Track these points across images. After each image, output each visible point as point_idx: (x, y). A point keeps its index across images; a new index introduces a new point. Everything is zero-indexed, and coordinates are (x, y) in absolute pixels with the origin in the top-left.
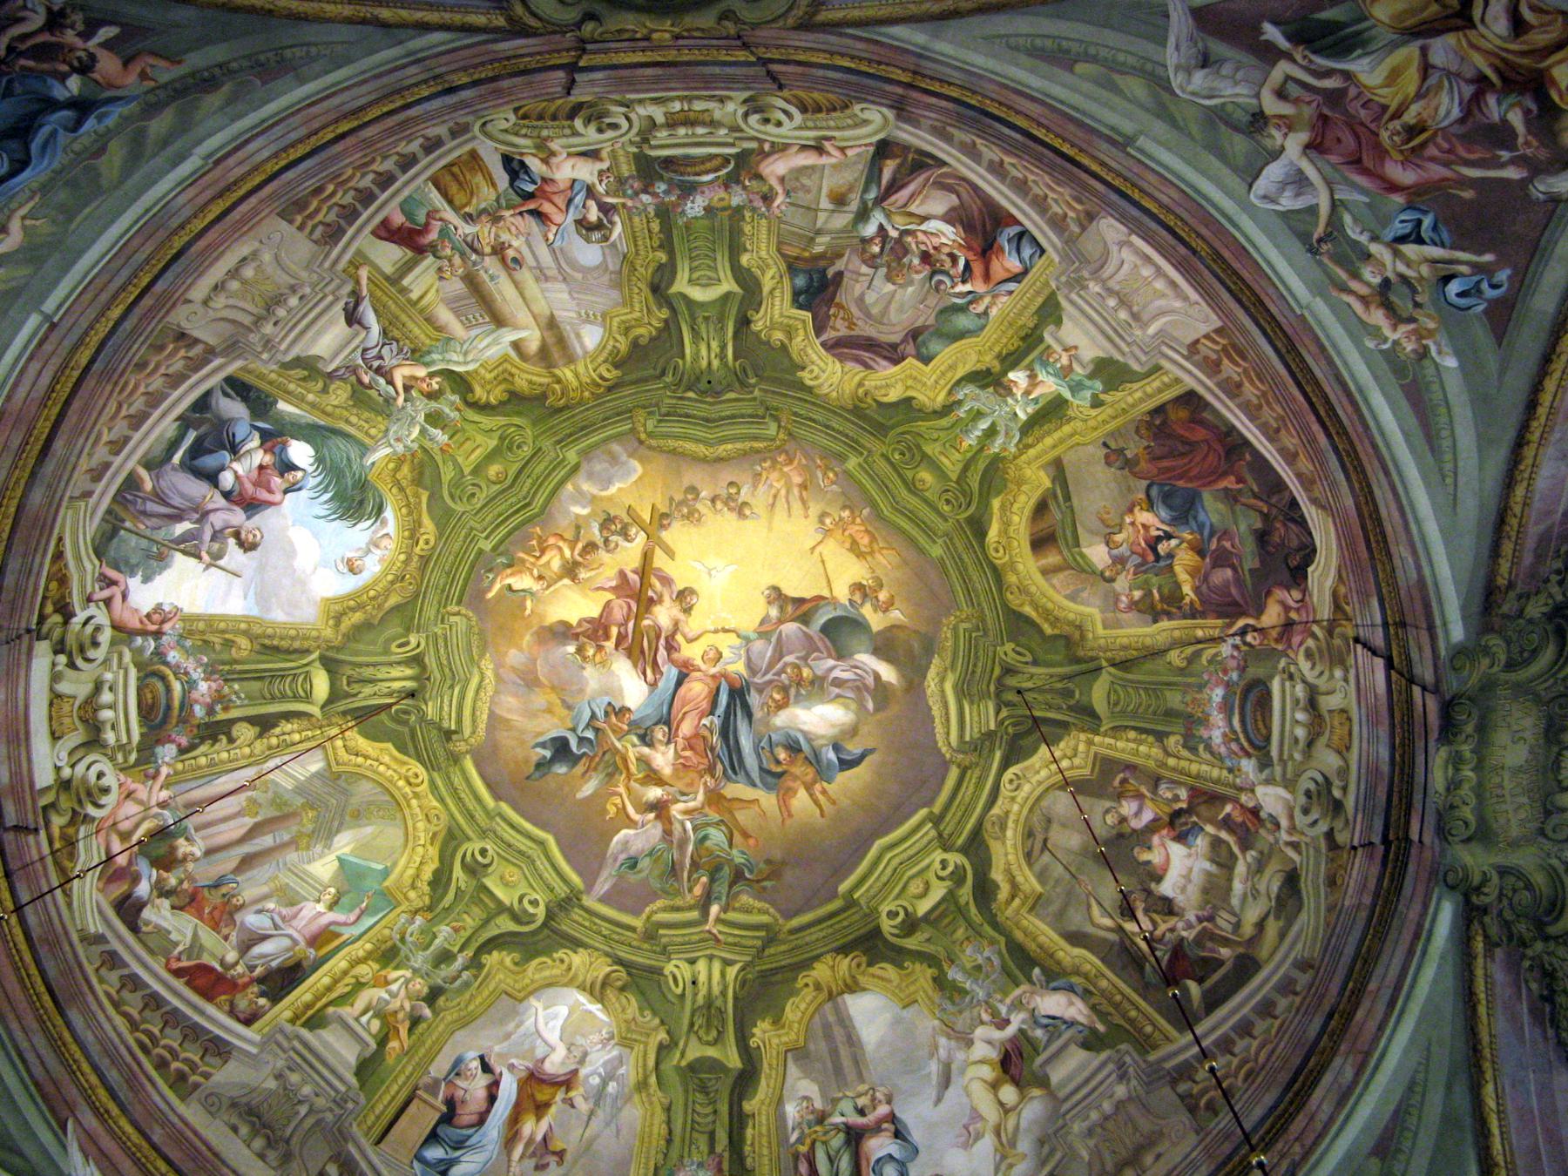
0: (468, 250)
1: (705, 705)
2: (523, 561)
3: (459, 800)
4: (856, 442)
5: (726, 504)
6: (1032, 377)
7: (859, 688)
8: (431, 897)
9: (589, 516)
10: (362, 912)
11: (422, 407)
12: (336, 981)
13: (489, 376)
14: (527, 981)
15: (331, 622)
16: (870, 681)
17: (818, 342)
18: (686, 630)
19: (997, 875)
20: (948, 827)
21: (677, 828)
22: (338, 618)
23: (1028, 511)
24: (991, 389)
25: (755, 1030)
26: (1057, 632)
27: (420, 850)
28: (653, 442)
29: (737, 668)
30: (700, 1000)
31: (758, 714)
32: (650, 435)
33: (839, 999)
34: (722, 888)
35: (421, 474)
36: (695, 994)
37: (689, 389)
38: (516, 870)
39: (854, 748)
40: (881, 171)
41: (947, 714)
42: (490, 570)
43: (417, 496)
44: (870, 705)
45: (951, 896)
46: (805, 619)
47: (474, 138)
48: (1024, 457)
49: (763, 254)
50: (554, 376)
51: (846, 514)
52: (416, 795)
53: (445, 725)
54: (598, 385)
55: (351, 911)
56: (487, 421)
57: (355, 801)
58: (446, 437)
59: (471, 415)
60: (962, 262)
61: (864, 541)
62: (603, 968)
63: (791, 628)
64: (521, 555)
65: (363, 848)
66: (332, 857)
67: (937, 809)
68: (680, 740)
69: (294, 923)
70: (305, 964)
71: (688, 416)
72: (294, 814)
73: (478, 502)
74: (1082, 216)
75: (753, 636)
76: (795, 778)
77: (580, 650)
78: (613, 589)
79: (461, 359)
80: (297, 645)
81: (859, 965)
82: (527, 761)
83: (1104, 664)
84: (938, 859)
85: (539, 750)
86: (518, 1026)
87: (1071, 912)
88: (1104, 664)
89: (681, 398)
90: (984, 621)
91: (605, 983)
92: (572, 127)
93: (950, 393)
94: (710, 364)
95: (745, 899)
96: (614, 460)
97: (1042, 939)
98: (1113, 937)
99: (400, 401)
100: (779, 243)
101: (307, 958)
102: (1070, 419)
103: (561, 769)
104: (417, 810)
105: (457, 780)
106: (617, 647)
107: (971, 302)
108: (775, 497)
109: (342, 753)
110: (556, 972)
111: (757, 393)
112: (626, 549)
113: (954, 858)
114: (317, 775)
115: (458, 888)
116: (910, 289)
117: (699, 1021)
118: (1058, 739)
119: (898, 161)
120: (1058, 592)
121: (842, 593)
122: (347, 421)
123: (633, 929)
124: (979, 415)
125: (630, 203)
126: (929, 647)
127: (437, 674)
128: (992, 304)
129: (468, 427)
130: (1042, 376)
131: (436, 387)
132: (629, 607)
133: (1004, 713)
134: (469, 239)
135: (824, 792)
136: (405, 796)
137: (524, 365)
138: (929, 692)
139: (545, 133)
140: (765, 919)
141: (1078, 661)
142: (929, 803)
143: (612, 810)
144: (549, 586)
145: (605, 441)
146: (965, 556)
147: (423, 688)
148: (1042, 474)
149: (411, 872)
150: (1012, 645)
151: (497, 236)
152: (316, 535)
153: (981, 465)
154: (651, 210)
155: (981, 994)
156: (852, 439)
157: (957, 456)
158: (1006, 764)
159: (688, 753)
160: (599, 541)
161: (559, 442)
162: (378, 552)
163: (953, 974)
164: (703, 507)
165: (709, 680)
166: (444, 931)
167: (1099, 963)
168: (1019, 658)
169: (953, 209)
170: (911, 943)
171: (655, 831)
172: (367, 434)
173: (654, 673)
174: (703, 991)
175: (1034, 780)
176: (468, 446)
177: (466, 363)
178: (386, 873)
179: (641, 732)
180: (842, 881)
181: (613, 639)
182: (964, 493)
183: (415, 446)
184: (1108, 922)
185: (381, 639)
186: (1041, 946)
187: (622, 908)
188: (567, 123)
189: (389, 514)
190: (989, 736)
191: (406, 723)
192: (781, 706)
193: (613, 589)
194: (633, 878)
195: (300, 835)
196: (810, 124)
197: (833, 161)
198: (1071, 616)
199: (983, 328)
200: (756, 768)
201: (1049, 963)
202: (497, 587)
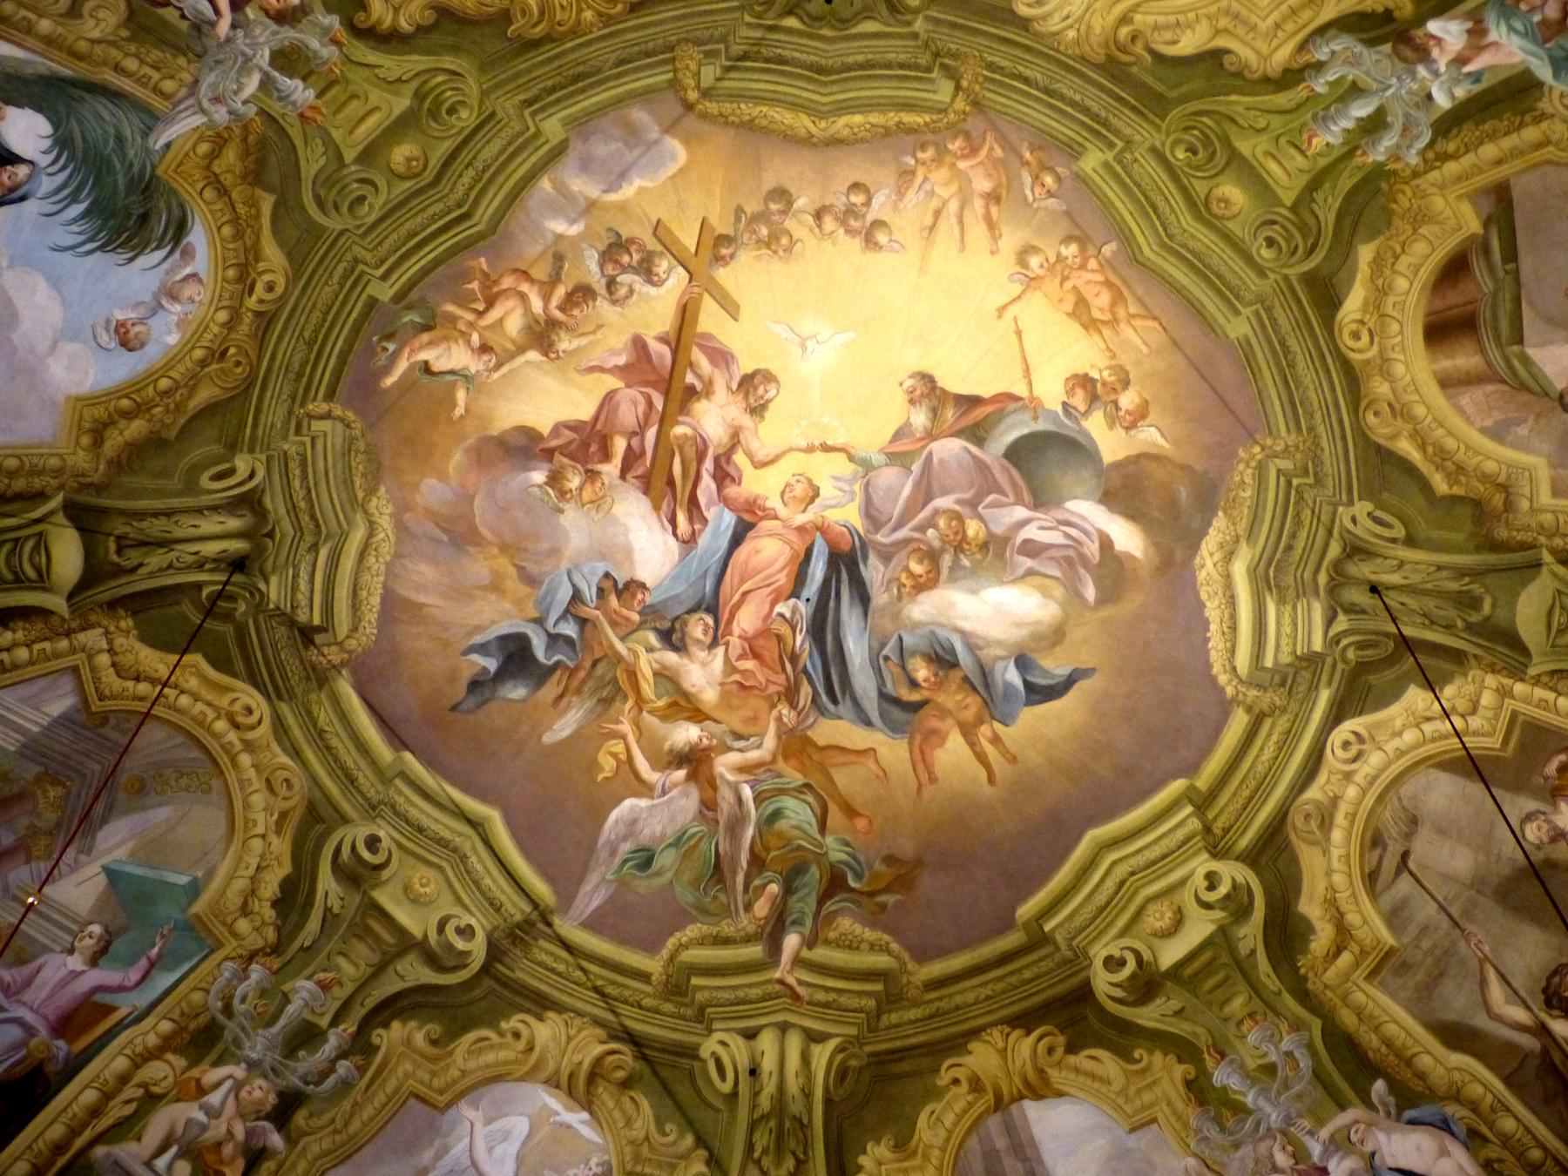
1: (783, 580)
2: (453, 319)
3: (327, 750)
5: (843, 222)
6: (1477, 32)
7: (1071, 561)
8: (279, 929)
9: (581, 237)
10: (152, 965)
11: (265, 38)
12: (107, 1097)
14: (456, 1073)
15: (86, 440)
16: (1092, 549)
18: (754, 445)
19: (1310, 907)
20: (1224, 809)
21: (726, 797)
22: (98, 433)
23: (1427, 272)
24: (1387, 48)
25: (863, 1160)
26: (1458, 491)
27: (257, 844)
28: (712, 107)
29: (846, 515)
30: (765, 1103)
31: (879, 598)
32: (706, 94)
33: (1014, 1108)
34: (804, 903)
35: (261, 163)
36: (756, 1094)
37: (790, 12)
38: (432, 874)
39: (1055, 666)
41: (1233, 618)
42: (389, 337)
43: (253, 203)
44: (1090, 593)
45: (1222, 938)
46: (977, 434)
48: (1434, 175)
51: (1071, 250)
52: (249, 746)
53: (302, 617)
55: (132, 963)
56: (391, 64)
57: (133, 764)
58: (310, 94)
59: (364, 52)
61: (1101, 301)
62: (591, 1047)
63: (950, 449)
64: (450, 308)
65: (152, 849)
66: (94, 868)
67: (1203, 781)
68: (734, 640)
69: (27, 996)
70: (50, 1068)
71: (782, 61)
72: (21, 796)
73: (369, 213)
75: (878, 459)
76: (944, 713)
77: (555, 479)
78: (621, 371)
80: (19, 485)
81: (1051, 1051)
82: (452, 677)
83: (1547, 557)
84: (1201, 871)
85: (475, 657)
86: (438, 1157)
87: (1448, 988)
88: (1547, 557)
89: (772, 28)
90: (1317, 460)
91: (593, 1076)
93: (1302, 47)
95: (846, 925)
96: (632, 134)
97: (1391, 1029)
98: (1529, 1042)
99: (224, 27)
101: (52, 1058)
102: (1543, 117)
103: (516, 692)
104: (251, 773)
105: (325, 716)
106: (623, 476)
108: (937, 214)
109: (110, 680)
110: (503, 1055)
111: (919, 25)
112: (647, 298)
113: (1232, 872)
114: (65, 720)
115: (327, 910)
117: (762, 1140)
118: (1447, 679)
120: (1468, 419)
121: (1051, 391)
122: (118, 68)
123: (645, 977)
124: (1355, 91)
126: (1209, 497)
127: (287, 525)
129: (355, 75)
130: (1497, 32)
132: (650, 404)
133: (1342, 623)
135: (996, 740)
136: (227, 748)
138: (1202, 576)
140: (882, 961)
141: (1496, 547)
142: (1191, 769)
143: (608, 764)
144: (498, 366)
145: (618, 102)
146: (1293, 343)
147: (259, 551)
148: (1467, 209)
149: (240, 884)
150: (1368, 506)
152: (55, 283)
153: (1346, 182)
155: (1274, 1118)
156: (1095, 117)
157: (1300, 161)
158: (1337, 716)
159: (749, 664)
160: (599, 284)
161: (528, 103)
162: (177, 308)
163: (1222, 1076)
164: (800, 226)
165: (793, 537)
166: (303, 988)
167: (1499, 1086)
168: (1379, 529)
170: (1148, 1016)
171: (686, 802)
172: (156, 90)
173: (691, 520)
174: (769, 1088)
175: (1390, 747)
176: (355, 108)
178: (195, 890)
179: (666, 625)
180: (1023, 899)
181: (617, 461)
182: (1303, 228)
183: (251, 110)
184: (1519, 1014)
185: (184, 464)
186: (1388, 1042)
187: (622, 940)
189: (197, 236)
190: (1311, 661)
191: (228, 617)
192: (922, 586)
193: (621, 371)
194: (644, 885)
195: (34, 832)
198: (1490, 466)
200: (874, 694)
201: (1405, 1074)
202: (402, 366)
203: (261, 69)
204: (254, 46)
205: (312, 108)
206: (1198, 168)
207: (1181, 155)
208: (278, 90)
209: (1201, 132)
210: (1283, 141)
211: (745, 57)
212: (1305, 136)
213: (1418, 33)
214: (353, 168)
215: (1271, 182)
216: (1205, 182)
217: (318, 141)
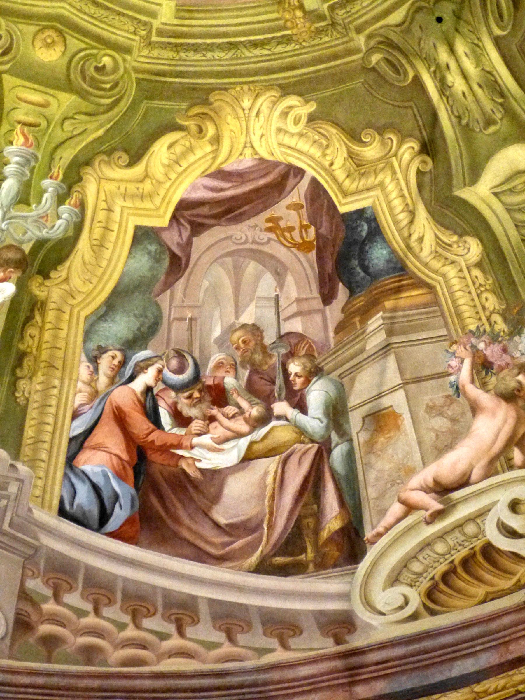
4: (176, 47)
17: (310, 172)
24: (27, 248)
40: (342, 503)
49: (451, 272)
60: (165, 418)
74: (34, 617)
93: (82, 206)
94: (452, 50)
100: (436, 302)
107: (123, 364)
111: (361, 40)
116: (217, 332)
119: (325, 534)
128: (91, 382)
156: (187, 47)
157: (20, 115)
169: (216, 498)
196: (471, 529)
197: (416, 481)
199: (87, 335)
206: (87, 58)
207: (106, 61)
209: (104, 89)
210: (44, 124)
212: (31, 138)
213: (15, 276)
215: (28, 84)
216: (74, 50)
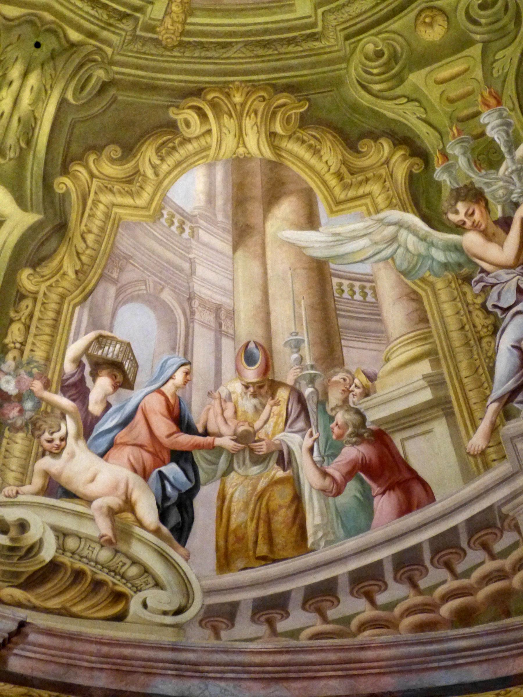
0: (311, 407)
13: (375, 188)
37: (73, 45)
47: (208, 592)
50: (275, 148)
54: (214, 105)
58: (484, 119)
79: (404, 234)
89: (92, 35)
92: (62, 548)
94: (25, 75)
125: (37, 386)
131: (461, 207)
134: (301, 424)
137: (312, 183)
139: (105, 555)
151: (257, 411)
154: (10, 363)
161: (313, 37)
177: (399, 224)
188: (65, 559)
203: (513, 158)
204: (509, 181)
205: (488, 106)
208: (508, 134)
211: (124, 16)
214: (478, 37)
217: (495, 75)
